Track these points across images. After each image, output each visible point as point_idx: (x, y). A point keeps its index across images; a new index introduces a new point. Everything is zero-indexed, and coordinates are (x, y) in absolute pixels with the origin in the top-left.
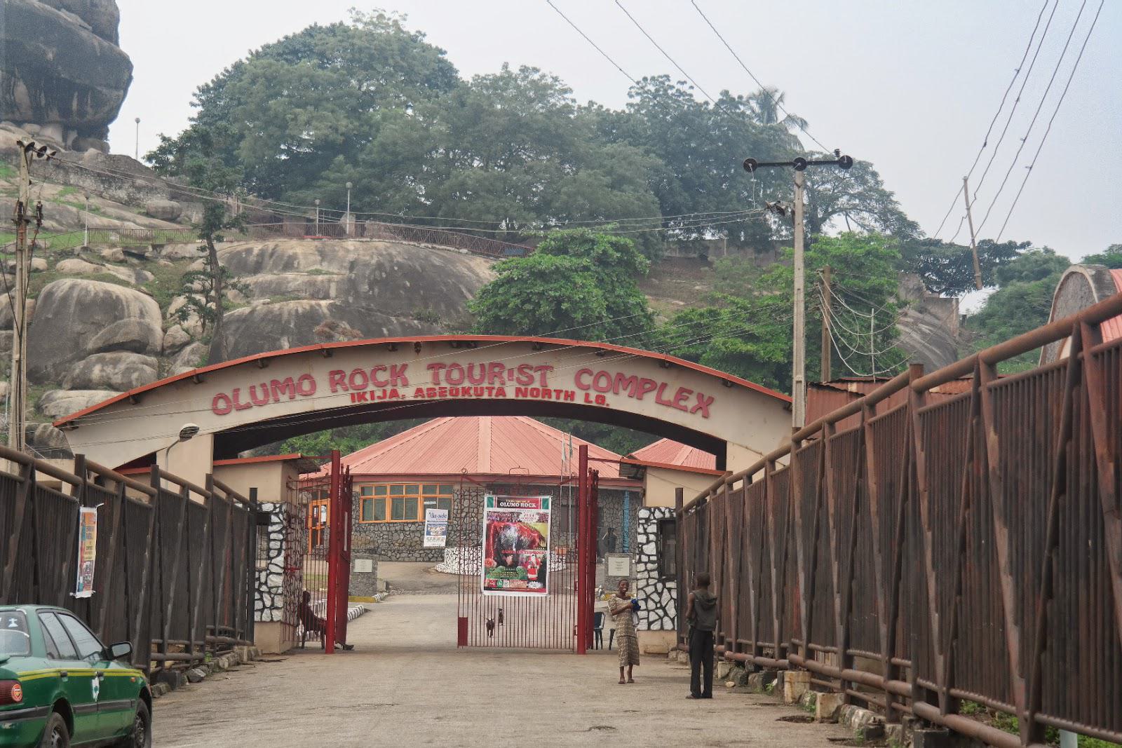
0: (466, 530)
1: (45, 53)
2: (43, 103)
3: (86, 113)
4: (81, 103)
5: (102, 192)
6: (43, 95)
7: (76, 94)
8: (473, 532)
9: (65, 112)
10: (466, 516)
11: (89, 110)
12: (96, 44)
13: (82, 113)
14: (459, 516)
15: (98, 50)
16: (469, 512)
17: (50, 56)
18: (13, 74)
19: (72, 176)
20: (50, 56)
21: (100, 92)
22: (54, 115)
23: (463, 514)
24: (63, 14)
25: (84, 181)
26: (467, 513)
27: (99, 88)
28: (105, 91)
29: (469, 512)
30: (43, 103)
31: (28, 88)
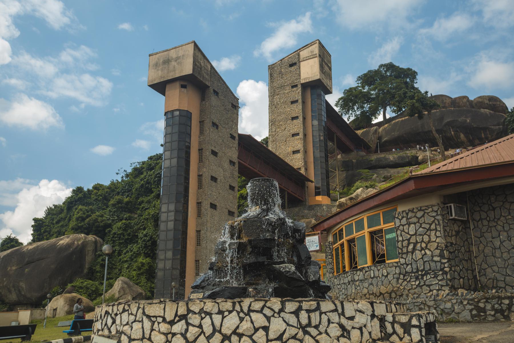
0: (418, 270)
1: (466, 121)
2: (471, 138)
7: (482, 132)
8: (427, 273)
10: (414, 249)
11: (489, 136)
12: (488, 113)
14: (405, 250)
15: (489, 115)
16: (417, 242)
17: (468, 121)
18: (457, 131)
20: (468, 121)
21: (490, 128)
23: (411, 247)
24: (482, 110)
26: (415, 244)
28: (493, 127)
29: (417, 242)
30: (471, 138)
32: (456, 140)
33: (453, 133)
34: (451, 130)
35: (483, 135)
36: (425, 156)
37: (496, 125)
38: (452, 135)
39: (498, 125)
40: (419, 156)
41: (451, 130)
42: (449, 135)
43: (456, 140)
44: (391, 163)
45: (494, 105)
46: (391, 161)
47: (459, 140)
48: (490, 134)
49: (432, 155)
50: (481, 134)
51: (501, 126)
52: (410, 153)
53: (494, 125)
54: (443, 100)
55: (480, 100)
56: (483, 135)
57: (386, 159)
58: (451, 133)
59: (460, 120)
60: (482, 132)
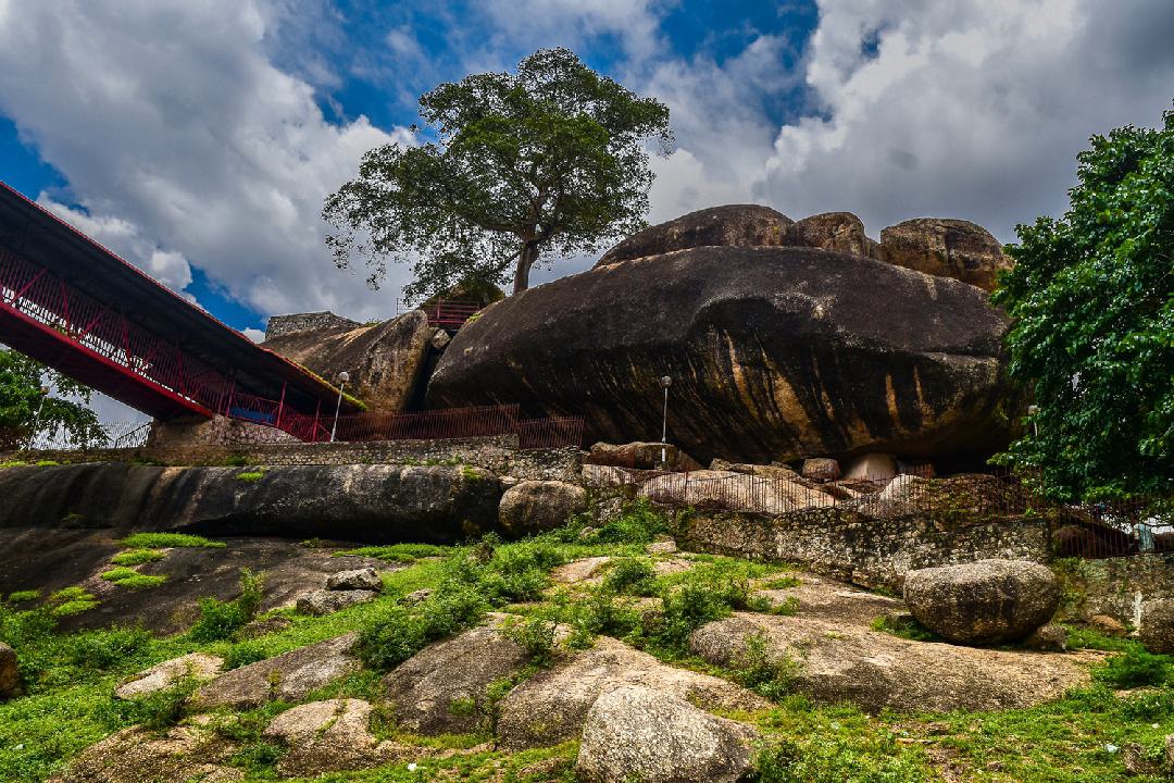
1: (809, 307)
3: (919, 414)
4: (905, 397)
5: (850, 569)
6: (824, 394)
7: (888, 379)
9: (878, 420)
13: (910, 417)
17: (819, 308)
19: (779, 537)
20: (819, 308)
21: (934, 363)
22: (859, 434)
25: (805, 544)
27: (933, 356)
31: (794, 388)
32: (755, 413)
33: (737, 370)
34: (732, 352)
35: (891, 399)
36: (537, 491)
37: (966, 353)
38: (732, 380)
39: (976, 354)
40: (508, 487)
41: (732, 352)
42: (717, 381)
43: (755, 413)
44: (338, 513)
45: (966, 261)
46: (346, 501)
47: (769, 415)
48: (927, 400)
49: (579, 490)
50: (886, 393)
51: (993, 362)
52: (463, 463)
53: (951, 351)
54: (749, 227)
55: (910, 235)
56: (891, 399)
57: (319, 480)
58: (729, 372)
59: (776, 302)
60: (888, 379)
